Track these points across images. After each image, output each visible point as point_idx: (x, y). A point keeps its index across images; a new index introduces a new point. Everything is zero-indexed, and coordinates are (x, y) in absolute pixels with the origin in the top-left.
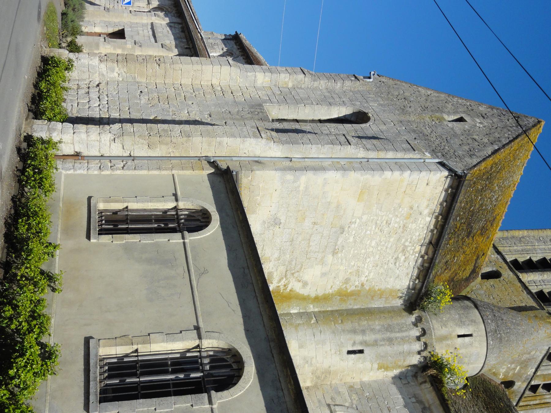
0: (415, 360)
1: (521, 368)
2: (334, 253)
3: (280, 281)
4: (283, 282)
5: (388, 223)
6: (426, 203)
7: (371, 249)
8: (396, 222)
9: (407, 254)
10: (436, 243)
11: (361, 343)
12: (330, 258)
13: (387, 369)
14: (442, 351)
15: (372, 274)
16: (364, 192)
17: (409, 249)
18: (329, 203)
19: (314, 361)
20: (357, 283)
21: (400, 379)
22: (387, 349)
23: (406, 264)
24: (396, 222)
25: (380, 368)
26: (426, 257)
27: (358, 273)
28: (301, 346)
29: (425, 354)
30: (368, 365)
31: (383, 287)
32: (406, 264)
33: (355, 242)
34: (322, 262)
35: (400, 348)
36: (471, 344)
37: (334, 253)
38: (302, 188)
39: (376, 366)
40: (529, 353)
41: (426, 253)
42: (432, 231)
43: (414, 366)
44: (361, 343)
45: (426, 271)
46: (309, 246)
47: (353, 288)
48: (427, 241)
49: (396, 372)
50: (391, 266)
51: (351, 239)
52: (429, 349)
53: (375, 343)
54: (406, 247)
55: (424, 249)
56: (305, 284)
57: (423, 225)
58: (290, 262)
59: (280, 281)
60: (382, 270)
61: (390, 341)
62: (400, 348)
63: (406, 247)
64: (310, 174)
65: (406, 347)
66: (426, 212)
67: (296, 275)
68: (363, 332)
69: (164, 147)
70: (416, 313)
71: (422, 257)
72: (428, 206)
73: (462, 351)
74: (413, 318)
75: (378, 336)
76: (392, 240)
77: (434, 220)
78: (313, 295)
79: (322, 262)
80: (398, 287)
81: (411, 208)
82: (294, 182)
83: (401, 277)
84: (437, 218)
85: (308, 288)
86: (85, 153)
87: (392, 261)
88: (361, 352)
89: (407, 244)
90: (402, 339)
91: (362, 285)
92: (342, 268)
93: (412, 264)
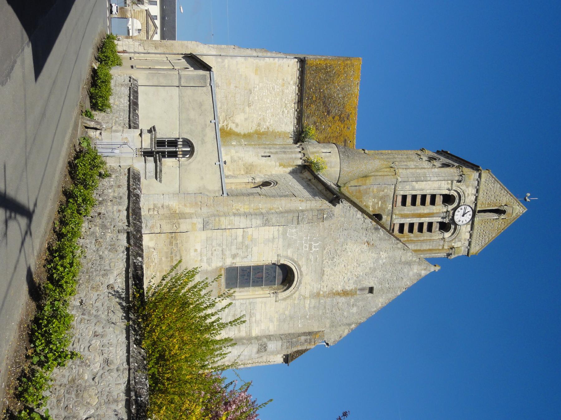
0: (300, 162)
1: (382, 203)
2: (249, 106)
3: (223, 122)
4: (225, 123)
5: (274, 89)
6: (290, 77)
7: (268, 105)
8: (278, 88)
9: (288, 109)
10: (300, 101)
11: (269, 152)
12: (247, 109)
13: (284, 166)
14: (313, 158)
15: (272, 121)
16: (257, 70)
17: (288, 105)
18: (241, 75)
19: (244, 159)
20: (265, 127)
21: (293, 173)
22: (284, 156)
23: (289, 115)
24: (278, 88)
25: (280, 165)
26: (298, 110)
27: (264, 120)
28: (236, 152)
29: (304, 158)
30: (273, 163)
31: (279, 130)
32: (289, 115)
33: (258, 99)
34: (244, 111)
35: (290, 156)
36: (331, 156)
37: (249, 106)
38: (226, 66)
39: (278, 164)
40: (383, 191)
41: (298, 108)
42: (297, 94)
43: (299, 166)
44: (269, 152)
45: (300, 119)
46: (235, 101)
47: (263, 130)
48: (297, 100)
49: (290, 169)
50: (281, 116)
51: (256, 98)
52: (306, 156)
53: (276, 153)
54: (286, 104)
55: (296, 105)
56: (237, 125)
57: (292, 90)
58: (227, 110)
59: (223, 122)
60: (276, 119)
61: (285, 152)
62: (290, 156)
63: (286, 104)
64: (229, 58)
65: (294, 156)
66: (292, 82)
67: (231, 119)
68: (270, 148)
69: (162, 48)
70: (299, 144)
71: (296, 111)
72: (292, 79)
73: (326, 159)
74: (298, 145)
75: (278, 150)
76: (278, 99)
77: (297, 88)
78: (242, 133)
79: (244, 111)
80: (288, 131)
81: (283, 80)
82: (222, 62)
83: (289, 126)
84: (298, 86)
85: (239, 127)
86: (128, 51)
87: (281, 113)
88: (269, 156)
89: (286, 102)
90: (291, 152)
91: (268, 128)
92: (255, 116)
93: (292, 115)
